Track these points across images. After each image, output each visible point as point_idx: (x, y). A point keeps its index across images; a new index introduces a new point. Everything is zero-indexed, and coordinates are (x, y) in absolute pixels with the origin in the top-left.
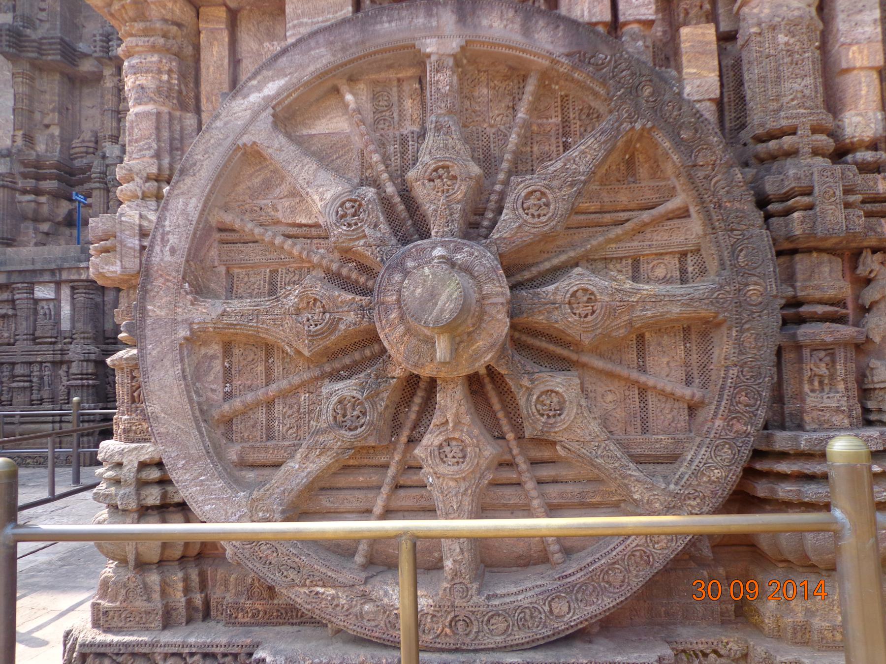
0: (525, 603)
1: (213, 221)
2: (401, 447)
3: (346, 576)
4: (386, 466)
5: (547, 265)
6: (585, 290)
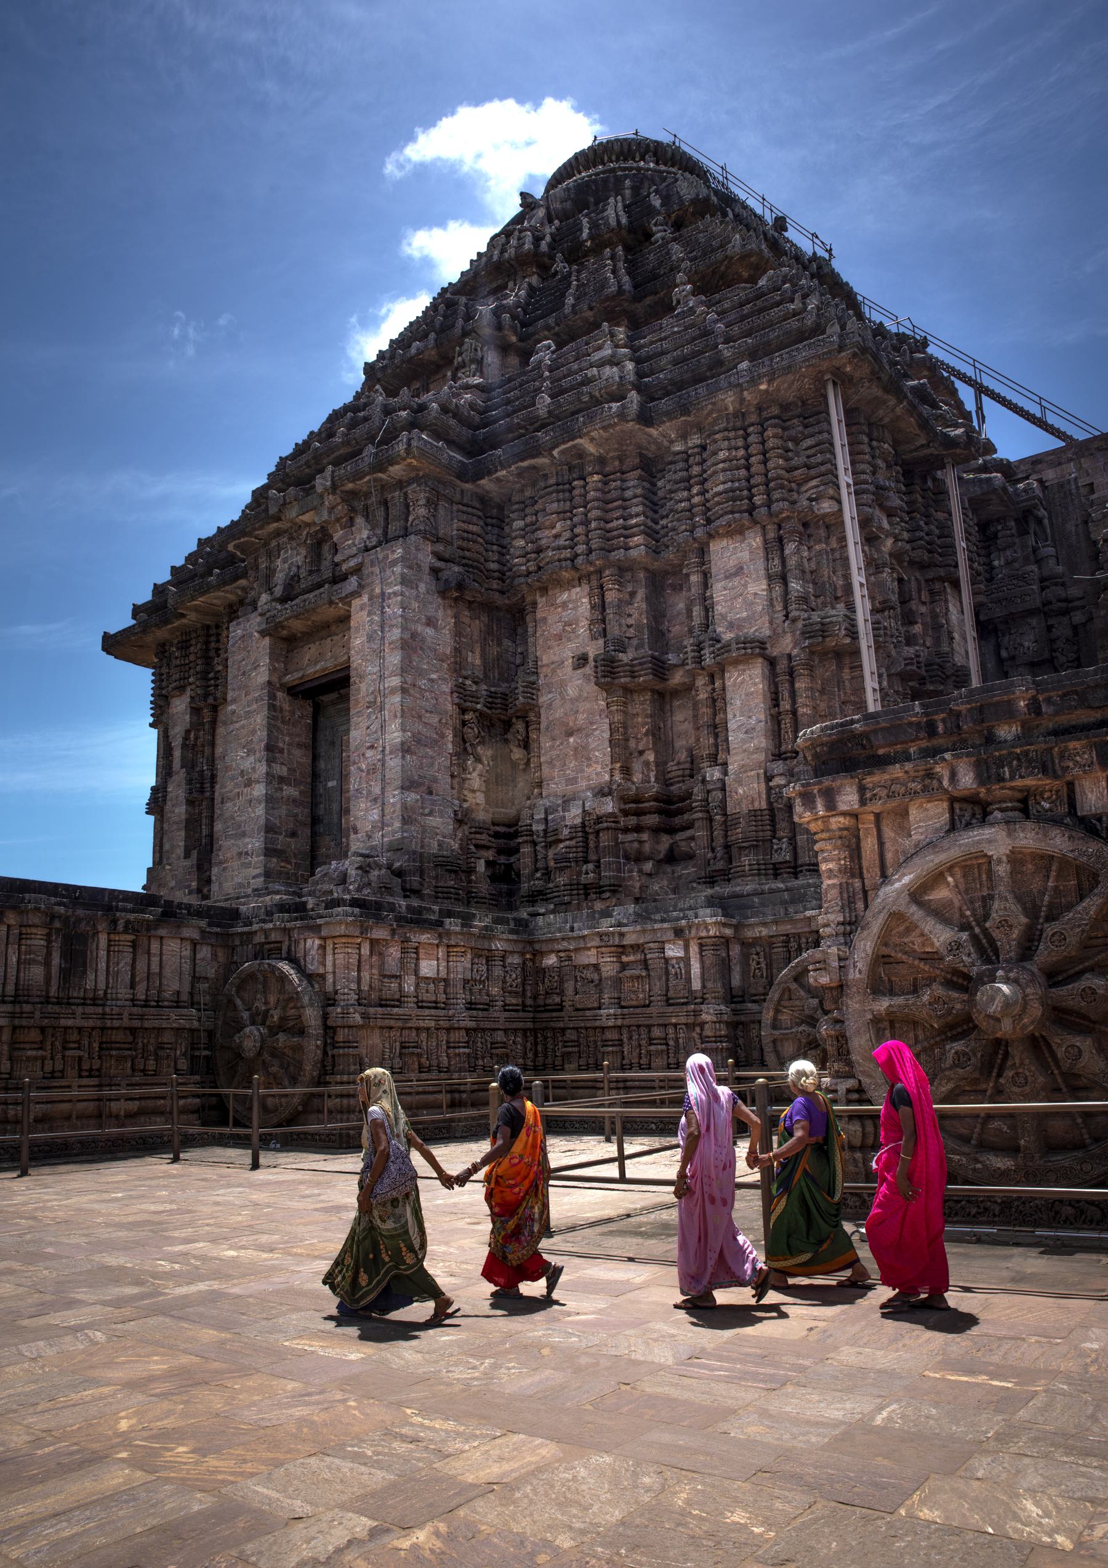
0: (1066, 1165)
1: (881, 953)
2: (993, 1079)
3: (966, 1149)
4: (985, 1091)
5: (1072, 972)
6: (1090, 988)
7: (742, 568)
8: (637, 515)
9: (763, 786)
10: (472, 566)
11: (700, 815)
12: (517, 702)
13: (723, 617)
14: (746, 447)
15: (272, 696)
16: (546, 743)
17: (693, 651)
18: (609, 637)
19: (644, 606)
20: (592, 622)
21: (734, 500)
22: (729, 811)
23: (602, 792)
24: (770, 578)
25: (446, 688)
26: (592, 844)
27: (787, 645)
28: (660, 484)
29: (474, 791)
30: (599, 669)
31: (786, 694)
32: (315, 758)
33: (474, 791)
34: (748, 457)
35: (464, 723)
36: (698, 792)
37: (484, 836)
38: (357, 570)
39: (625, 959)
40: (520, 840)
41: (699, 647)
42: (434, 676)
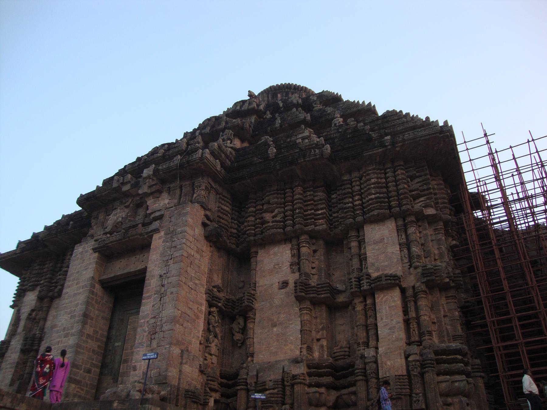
7: (384, 239)
8: (322, 209)
9: (404, 360)
10: (224, 228)
11: (361, 377)
12: (243, 305)
13: (373, 264)
14: (386, 178)
15: (93, 286)
16: (258, 331)
17: (355, 281)
18: (302, 272)
19: (322, 258)
20: (292, 264)
21: (381, 202)
22: (381, 375)
23: (296, 361)
24: (400, 245)
25: (203, 290)
26: (288, 393)
27: (410, 281)
28: (333, 196)
29: (211, 355)
30: (298, 288)
31: (413, 308)
32: (110, 328)
33: (211, 355)
34: (387, 183)
35: (210, 313)
36: (359, 364)
37: (216, 383)
38: (160, 217)
40: (239, 388)
41: (359, 279)
42: (197, 282)
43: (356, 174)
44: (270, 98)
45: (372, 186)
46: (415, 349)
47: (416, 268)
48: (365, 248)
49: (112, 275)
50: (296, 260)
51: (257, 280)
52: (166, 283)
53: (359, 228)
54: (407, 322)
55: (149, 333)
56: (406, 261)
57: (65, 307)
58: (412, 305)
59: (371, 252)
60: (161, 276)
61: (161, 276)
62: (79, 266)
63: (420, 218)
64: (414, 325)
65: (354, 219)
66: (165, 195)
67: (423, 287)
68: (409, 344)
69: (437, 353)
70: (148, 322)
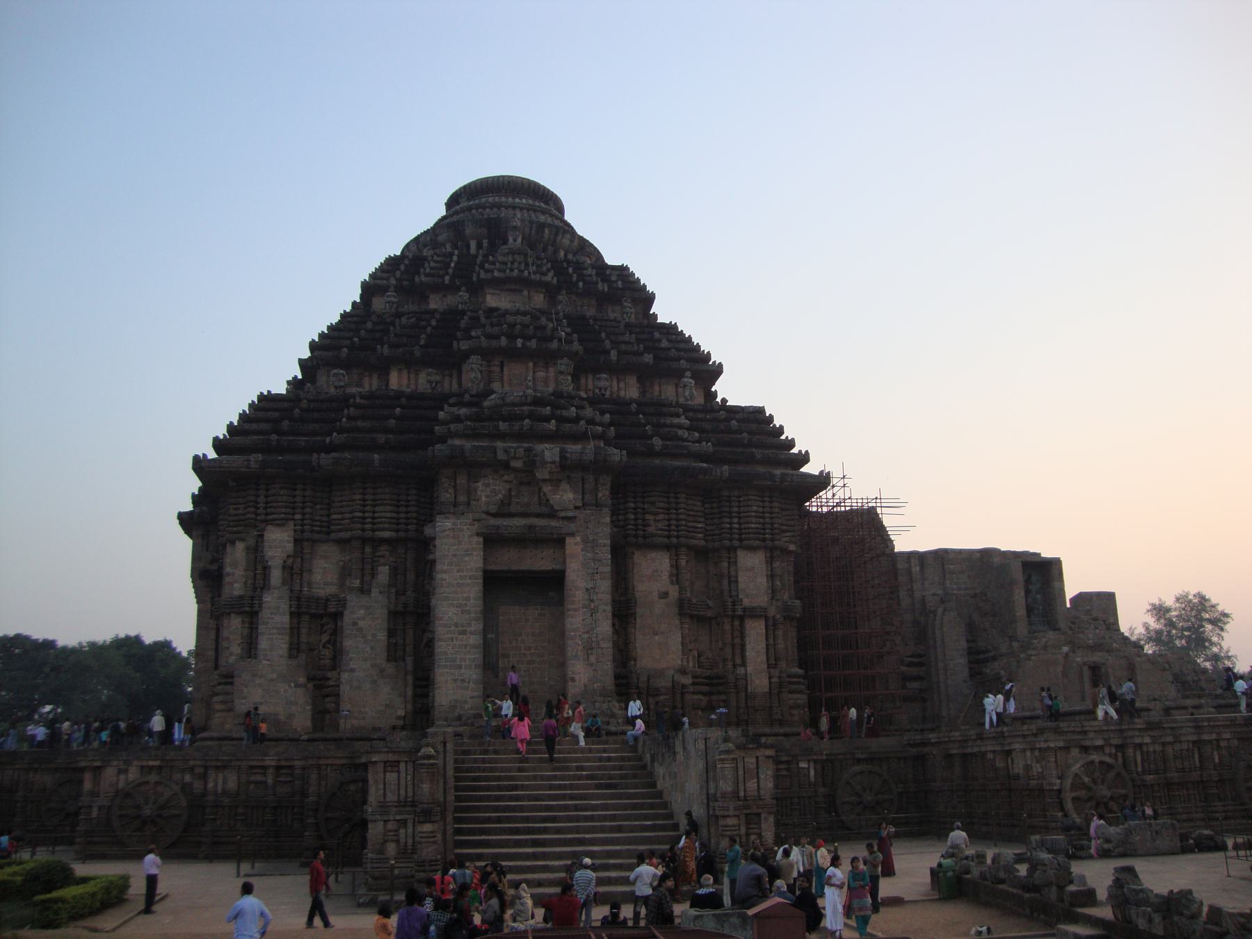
20: (671, 575)
22: (749, 690)
23: (683, 671)
27: (772, 612)
39: (780, 767)
41: (734, 604)
43: (736, 493)
44: (533, 232)
45: (753, 514)
46: (775, 672)
47: (777, 600)
48: (736, 571)
49: (505, 568)
50: (674, 571)
51: (635, 583)
52: (595, 598)
53: (732, 549)
54: (767, 645)
55: (584, 648)
56: (770, 592)
57: (447, 597)
58: (771, 632)
59: (742, 578)
60: (587, 590)
61: (587, 590)
62: (455, 547)
63: (785, 551)
64: (771, 651)
65: (731, 540)
66: (565, 485)
67: (782, 619)
68: (769, 666)
69: (789, 676)
70: (580, 636)
